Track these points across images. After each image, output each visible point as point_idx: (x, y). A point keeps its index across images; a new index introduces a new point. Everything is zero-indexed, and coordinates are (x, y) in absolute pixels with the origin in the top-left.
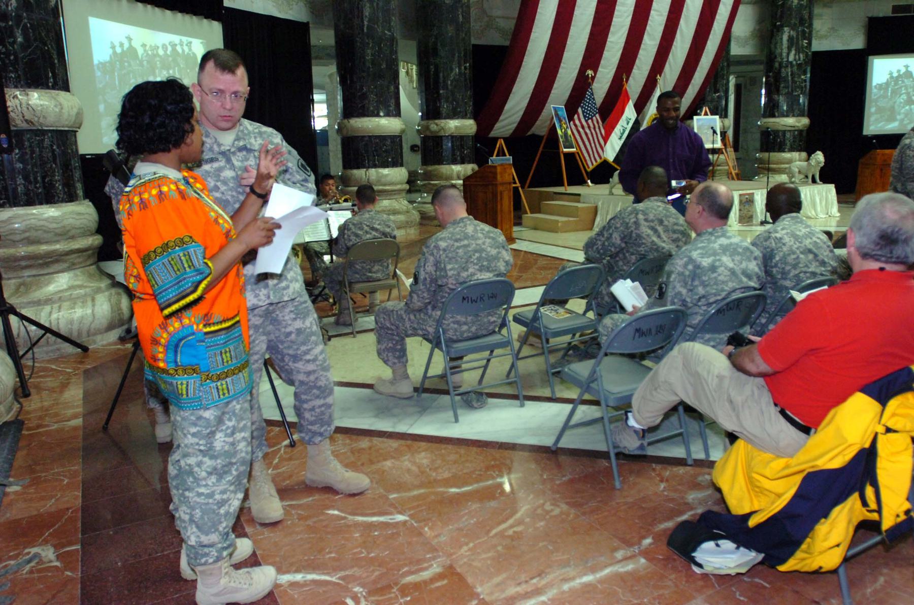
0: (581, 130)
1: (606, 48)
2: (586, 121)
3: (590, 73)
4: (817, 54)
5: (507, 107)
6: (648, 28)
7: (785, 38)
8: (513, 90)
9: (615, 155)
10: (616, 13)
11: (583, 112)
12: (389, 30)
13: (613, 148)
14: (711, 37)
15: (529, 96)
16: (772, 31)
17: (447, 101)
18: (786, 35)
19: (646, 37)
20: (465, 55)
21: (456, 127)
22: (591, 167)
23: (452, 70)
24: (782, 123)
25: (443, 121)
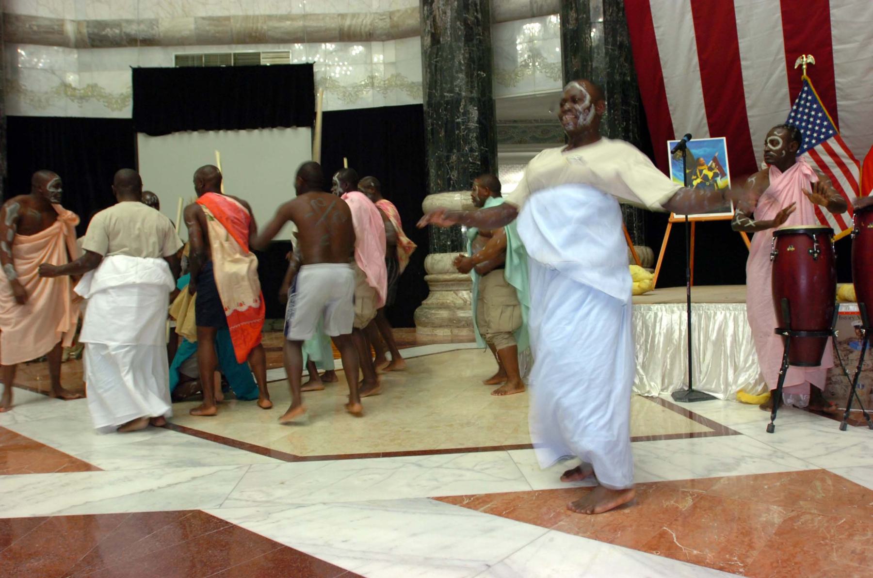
12: (451, 91)
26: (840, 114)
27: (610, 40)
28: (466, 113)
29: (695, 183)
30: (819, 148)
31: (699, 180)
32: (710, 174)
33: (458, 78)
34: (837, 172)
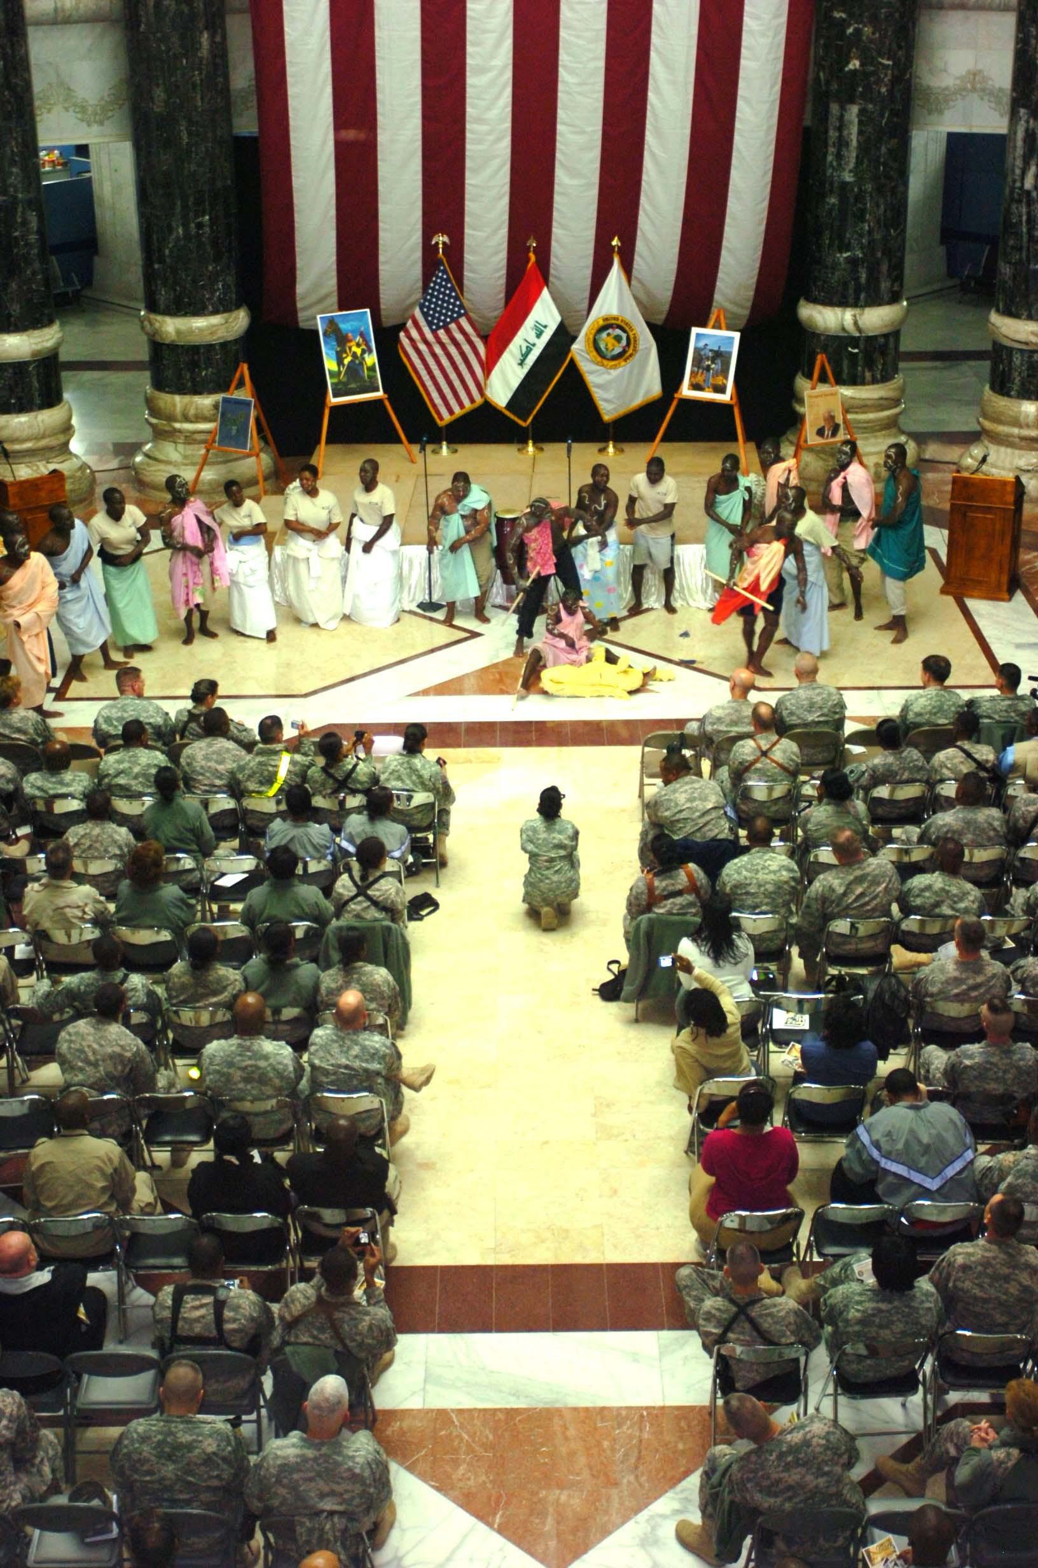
0: (422, 347)
2: (434, 332)
3: (441, 239)
5: (300, 289)
6: (558, 155)
9: (510, 395)
10: (468, 135)
11: (425, 315)
13: (506, 382)
14: (734, 161)
17: (165, 285)
19: (560, 174)
20: (199, 202)
21: (178, 332)
22: (447, 418)
23: (170, 229)
24: (1004, 330)
25: (159, 318)
26: (466, 282)
27: (210, 135)
28: (25, 223)
29: (346, 361)
30: (453, 326)
31: (349, 359)
32: (358, 351)
33: (11, 173)
34: (466, 348)
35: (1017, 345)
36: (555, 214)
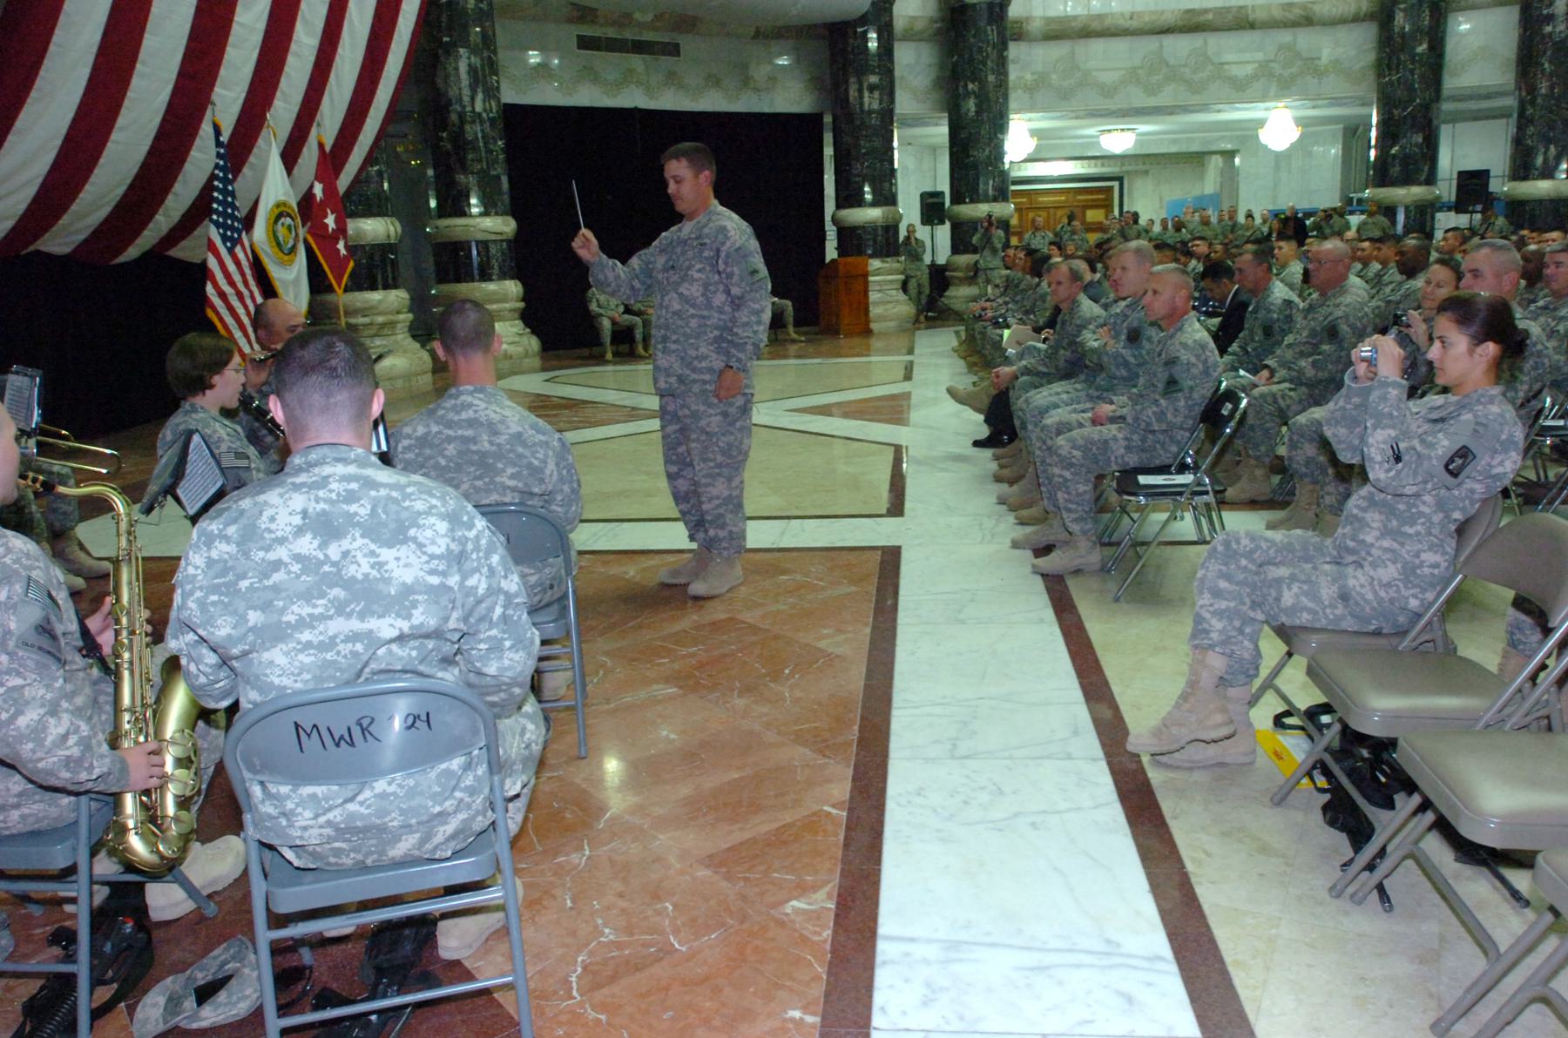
1: (231, 39)
4: (506, 105)
7: (463, 67)
8: (19, 124)
15: (59, 142)
16: (436, 56)
18: (464, 62)
35: (494, 237)
36: (283, 80)
